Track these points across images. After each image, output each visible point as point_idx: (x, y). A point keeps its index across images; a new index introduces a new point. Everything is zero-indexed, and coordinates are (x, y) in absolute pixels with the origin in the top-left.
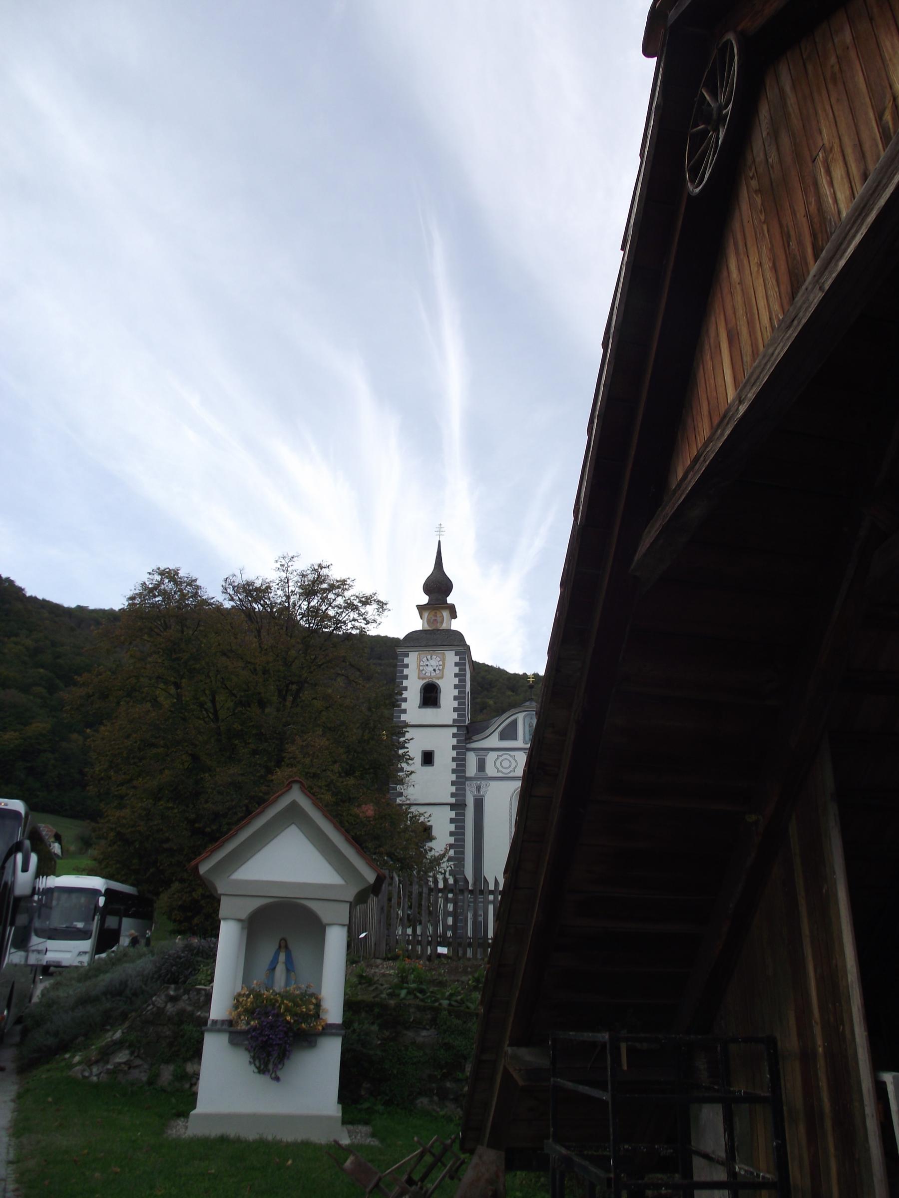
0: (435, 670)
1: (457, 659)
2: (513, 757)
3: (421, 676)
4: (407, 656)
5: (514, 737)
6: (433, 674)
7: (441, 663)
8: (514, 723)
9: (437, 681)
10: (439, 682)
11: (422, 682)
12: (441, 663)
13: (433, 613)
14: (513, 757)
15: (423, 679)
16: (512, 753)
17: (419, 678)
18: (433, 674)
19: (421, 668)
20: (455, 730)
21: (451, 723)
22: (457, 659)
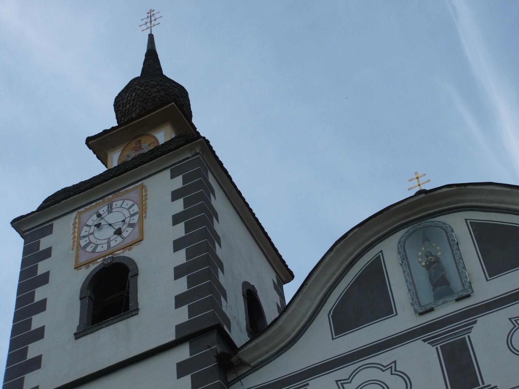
0: (118, 232)
1: (178, 183)
2: (392, 368)
3: (83, 259)
4: (48, 230)
5: (385, 309)
6: (116, 241)
7: (136, 209)
8: (376, 272)
9: (127, 254)
10: (132, 254)
11: (85, 273)
12: (136, 209)
13: (133, 144)
14: (392, 368)
15: (87, 264)
16: (384, 358)
17: (77, 268)
18: (116, 241)
19: (83, 243)
20: (183, 353)
21: (172, 337)
22: (178, 183)
